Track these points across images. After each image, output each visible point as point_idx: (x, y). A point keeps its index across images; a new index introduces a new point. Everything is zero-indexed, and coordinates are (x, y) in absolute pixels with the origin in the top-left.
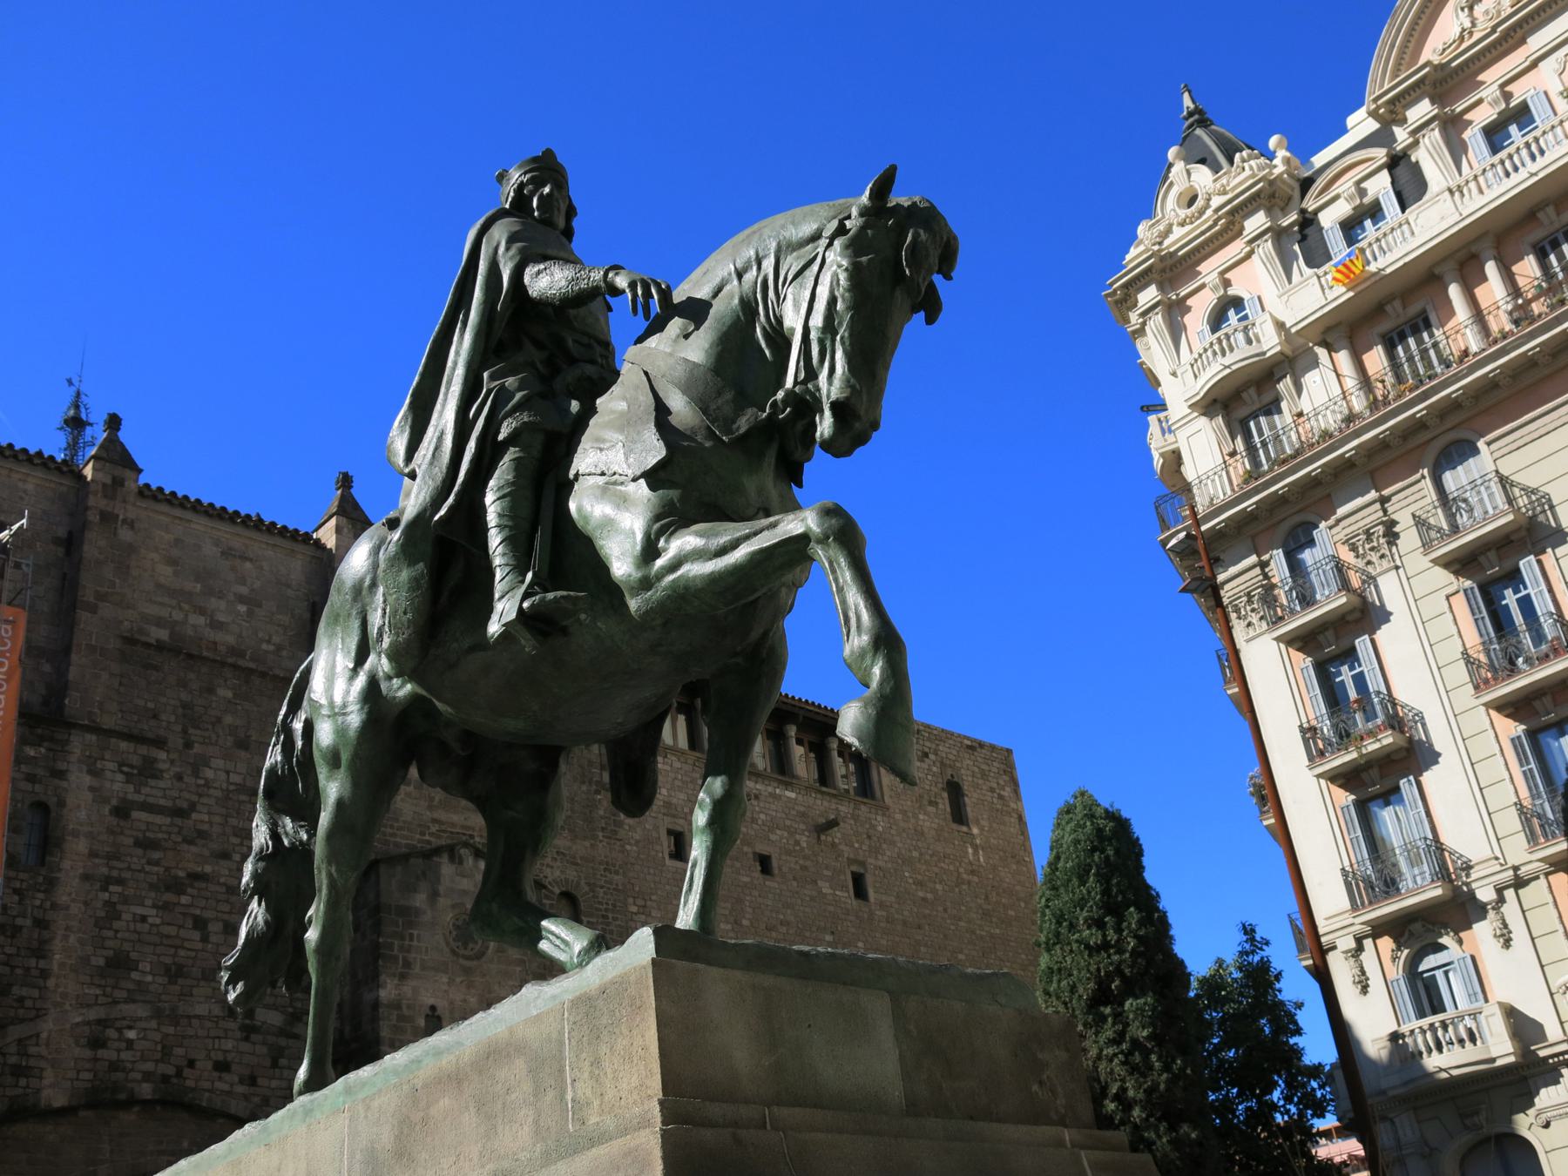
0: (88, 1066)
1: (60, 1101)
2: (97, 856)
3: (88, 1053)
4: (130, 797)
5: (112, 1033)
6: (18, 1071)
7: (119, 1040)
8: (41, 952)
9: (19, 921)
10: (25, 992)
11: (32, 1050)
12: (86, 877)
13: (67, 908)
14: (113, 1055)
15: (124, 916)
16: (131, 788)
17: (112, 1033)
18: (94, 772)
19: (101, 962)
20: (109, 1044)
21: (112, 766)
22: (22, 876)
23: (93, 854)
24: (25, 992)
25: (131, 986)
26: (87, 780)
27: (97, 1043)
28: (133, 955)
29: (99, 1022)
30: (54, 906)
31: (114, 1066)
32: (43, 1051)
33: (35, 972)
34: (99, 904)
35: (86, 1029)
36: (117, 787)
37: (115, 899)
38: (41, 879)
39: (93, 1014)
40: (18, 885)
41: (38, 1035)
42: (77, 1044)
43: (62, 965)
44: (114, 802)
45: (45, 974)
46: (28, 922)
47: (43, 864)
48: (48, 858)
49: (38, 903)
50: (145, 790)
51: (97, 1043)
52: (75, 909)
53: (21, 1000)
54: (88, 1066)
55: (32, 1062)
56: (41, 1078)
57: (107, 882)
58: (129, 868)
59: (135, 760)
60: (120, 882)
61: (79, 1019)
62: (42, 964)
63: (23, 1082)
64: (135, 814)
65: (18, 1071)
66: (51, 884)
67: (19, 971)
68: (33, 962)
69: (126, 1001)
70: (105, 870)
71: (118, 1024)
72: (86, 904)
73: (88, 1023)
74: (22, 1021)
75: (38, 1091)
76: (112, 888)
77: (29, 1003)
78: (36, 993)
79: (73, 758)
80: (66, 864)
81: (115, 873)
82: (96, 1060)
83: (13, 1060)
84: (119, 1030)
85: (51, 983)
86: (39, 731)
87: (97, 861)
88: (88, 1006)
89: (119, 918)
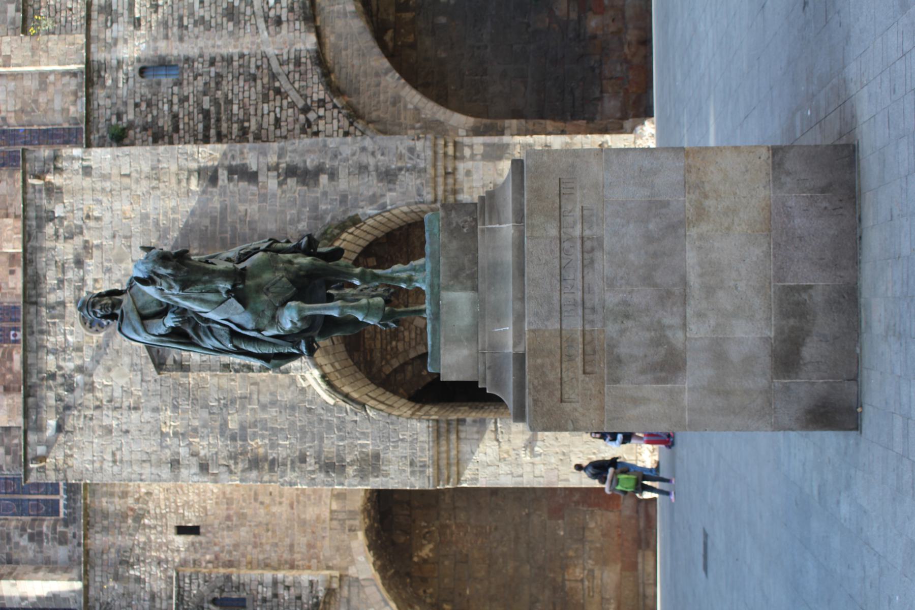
0: (292, 24)
1: (312, 39)
2: (167, 35)
3: (285, 26)
4: (126, 20)
5: (272, 13)
6: (298, 63)
7: (275, 8)
8: (229, 60)
9: (213, 74)
10: (253, 66)
11: (285, 57)
12: (181, 39)
13: (201, 48)
14: (285, 11)
15: (202, 13)
16: (121, 19)
17: (272, 13)
18: (115, 41)
19: (231, 24)
20: (278, 13)
21: (108, 32)
22: (185, 76)
23: (166, 37)
24: (253, 66)
25: (243, 5)
26: (120, 45)
27: (278, 22)
28: (225, 5)
29: (266, 22)
30: (201, 56)
31: (291, 9)
32: (285, 51)
33: (241, 62)
34: (196, 30)
35: (270, 28)
36: (121, 28)
37: (192, 21)
38: (186, 66)
39: (262, 25)
40: (191, 78)
41: (277, 55)
42: (280, 32)
43: (235, 47)
44: (132, 28)
45: (242, 56)
46: (213, 69)
47: (176, 65)
48: (173, 63)
49: (200, 66)
50: (120, 10)
51: (278, 22)
52: (201, 43)
53: (258, 67)
54: (292, 24)
55: (292, 56)
56: (300, 51)
57: (181, 26)
58: (172, 15)
59: (102, 18)
60: (181, 19)
61: (266, 33)
62: (236, 58)
63: (303, 60)
64: (137, 15)
65: (298, 63)
66: (187, 59)
67: (241, 71)
68: (235, 64)
69: (252, 7)
70: (175, 29)
71: (266, 10)
72: (197, 37)
73: (267, 28)
74: (269, 64)
75: (308, 51)
76: (185, 23)
77: (259, 63)
78: (253, 60)
79: (108, 57)
80: (175, 53)
81: (176, 22)
82: (288, 20)
83: (291, 67)
84: (270, 9)
85: (246, 52)
86: (95, 79)
87: (170, 34)
88: (257, 28)
89: (203, 17)
